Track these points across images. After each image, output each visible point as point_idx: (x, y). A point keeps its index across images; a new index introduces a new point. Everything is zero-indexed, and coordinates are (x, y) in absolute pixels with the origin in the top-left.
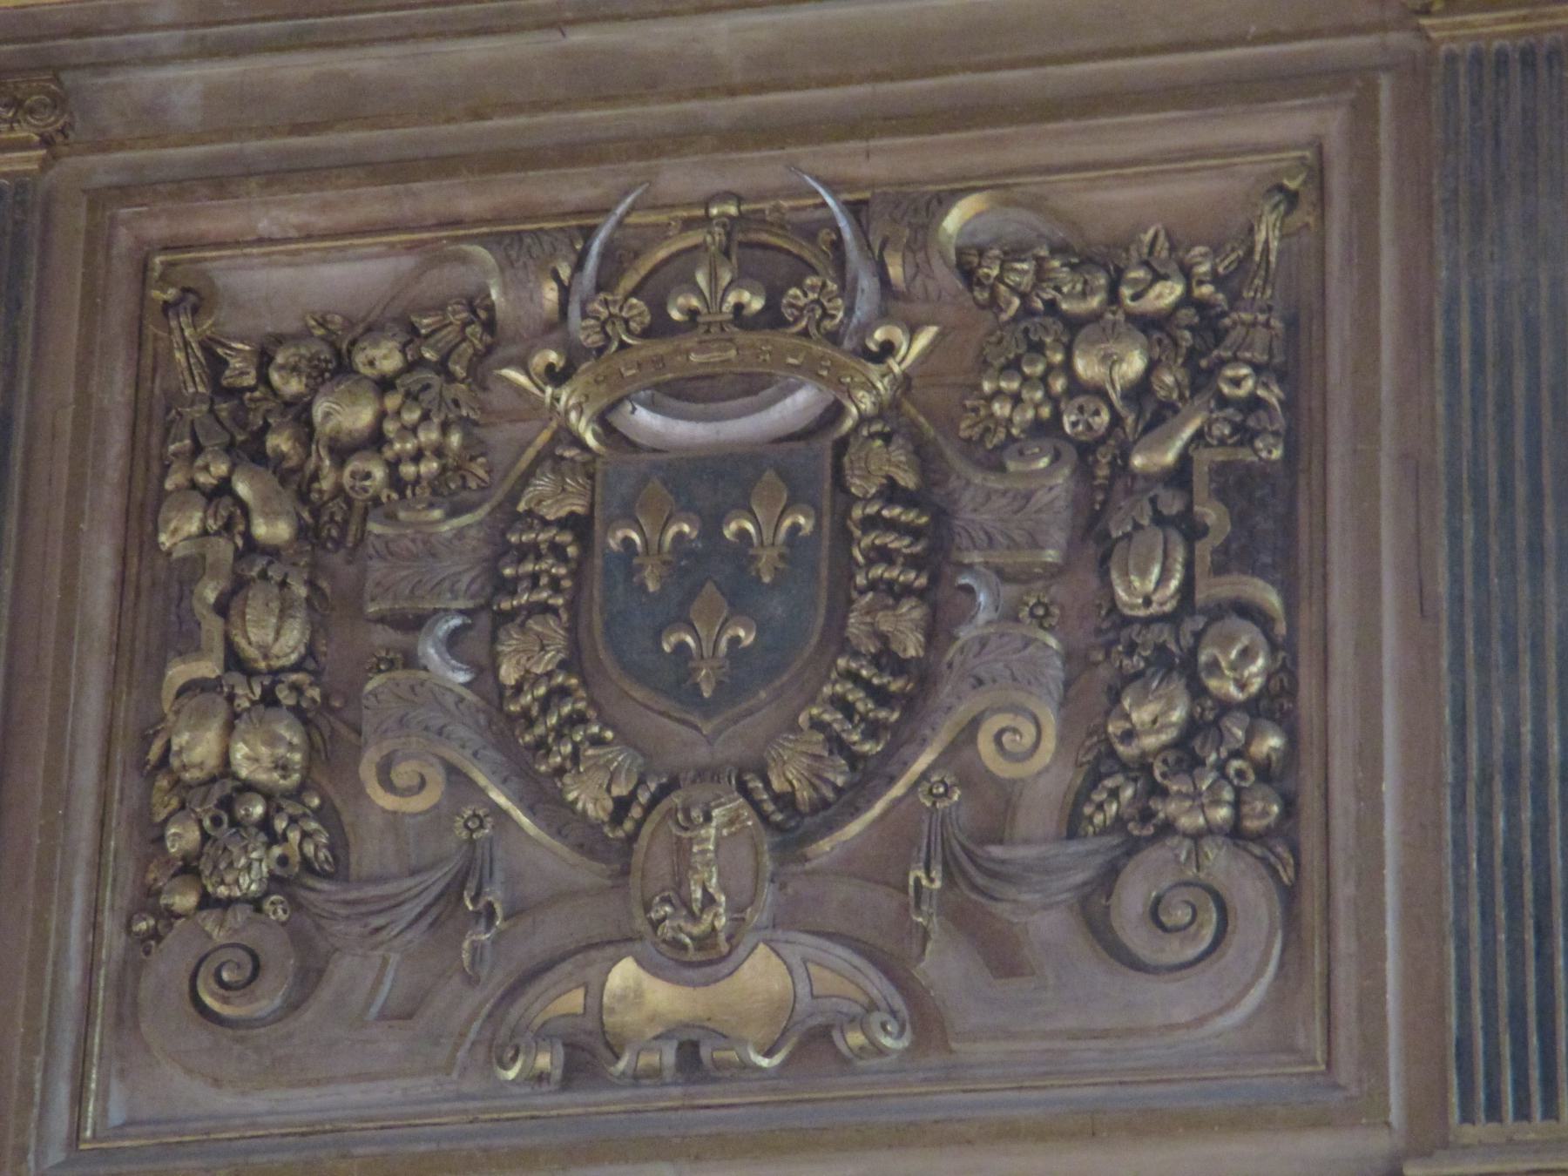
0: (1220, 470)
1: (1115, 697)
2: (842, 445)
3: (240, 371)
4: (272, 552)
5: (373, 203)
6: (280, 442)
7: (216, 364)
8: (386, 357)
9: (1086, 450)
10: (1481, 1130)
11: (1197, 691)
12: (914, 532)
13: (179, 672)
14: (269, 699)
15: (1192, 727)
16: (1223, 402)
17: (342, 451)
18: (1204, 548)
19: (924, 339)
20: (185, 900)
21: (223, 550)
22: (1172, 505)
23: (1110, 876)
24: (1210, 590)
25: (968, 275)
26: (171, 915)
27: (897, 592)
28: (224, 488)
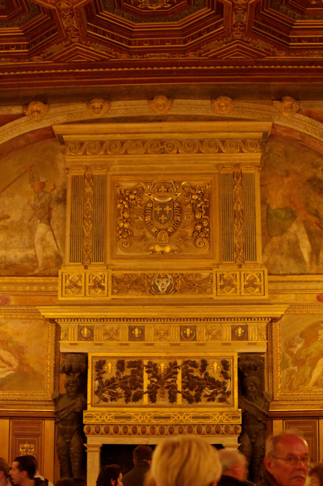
0: (204, 207)
1: (196, 225)
2: (173, 202)
3: (123, 192)
4: (126, 208)
5: (133, 178)
6: (127, 199)
7: (121, 192)
8: (135, 192)
9: (193, 204)
10: (224, 262)
11: (202, 225)
12: (179, 210)
13: (119, 218)
14: (127, 221)
15: (202, 228)
16: (204, 201)
17: (132, 200)
18: (203, 214)
19: (180, 193)
20: (121, 237)
21: (122, 208)
22: (200, 210)
23: (196, 240)
24: (203, 217)
25: (183, 188)
26: (120, 239)
27: (178, 215)
28: (122, 203)
